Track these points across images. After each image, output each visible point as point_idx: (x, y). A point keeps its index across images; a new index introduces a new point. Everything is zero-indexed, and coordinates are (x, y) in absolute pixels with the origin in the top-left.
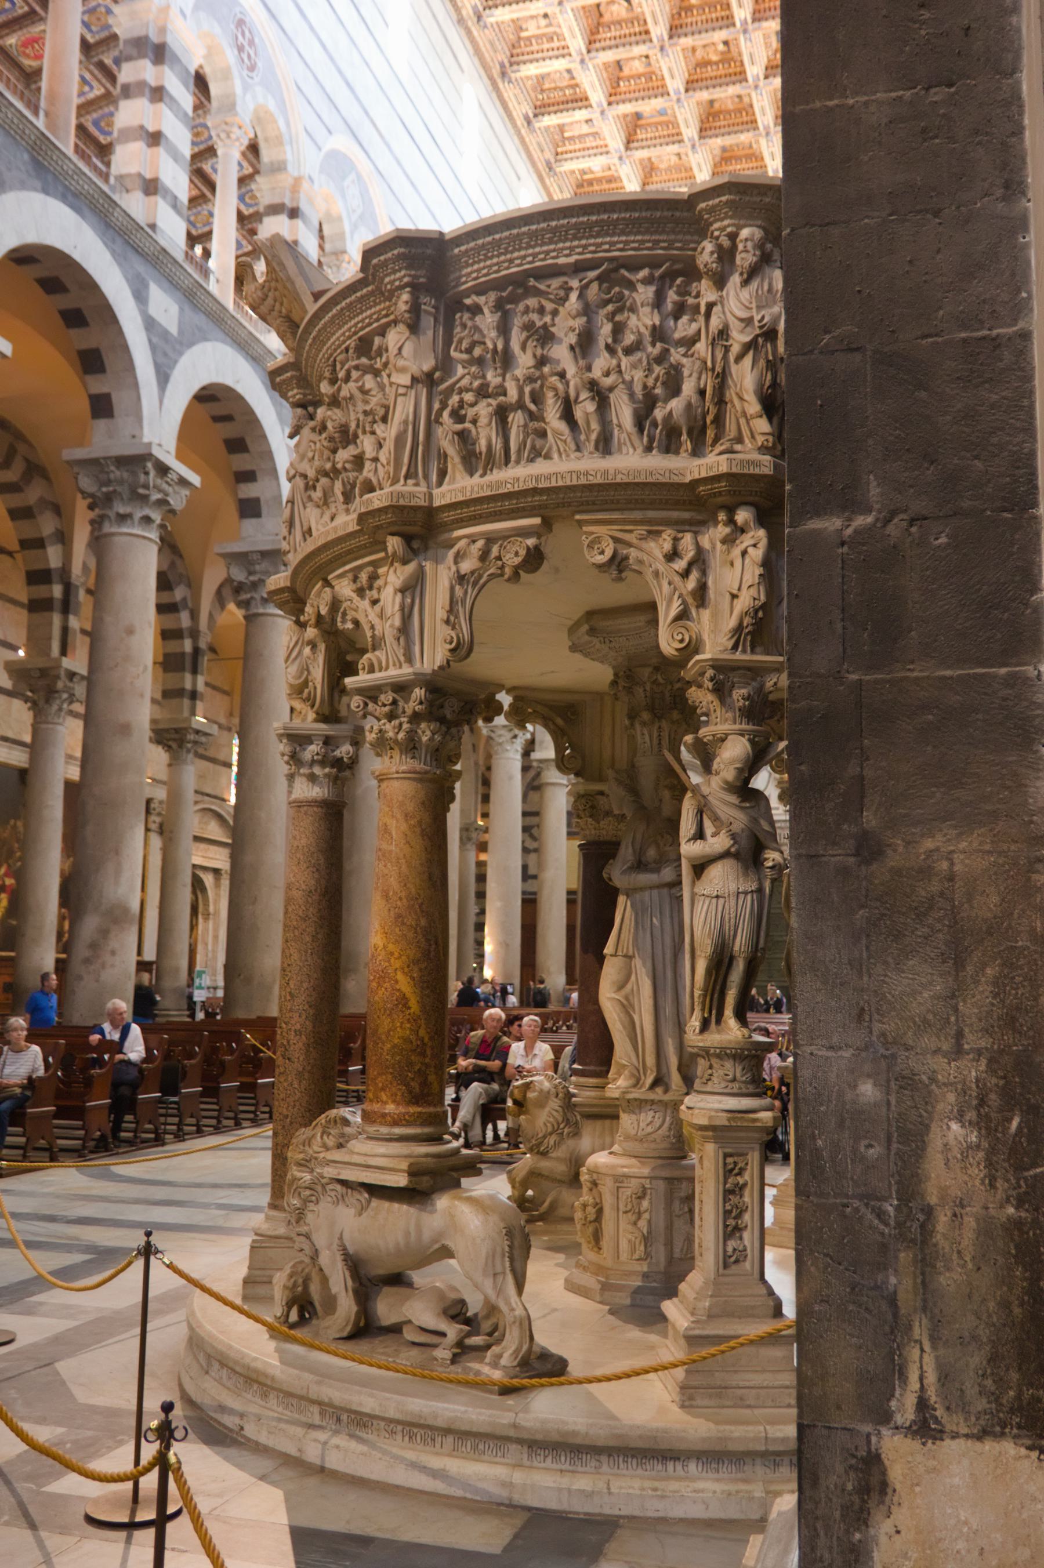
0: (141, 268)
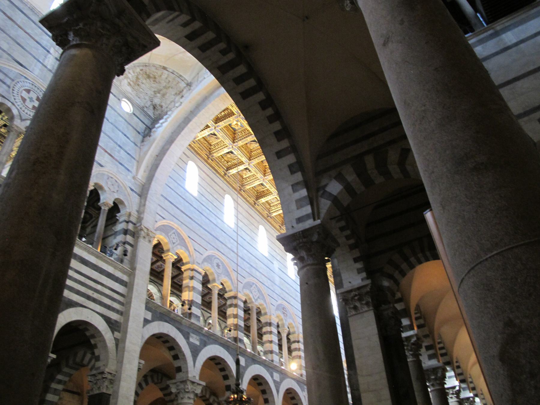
0: (271, 370)
